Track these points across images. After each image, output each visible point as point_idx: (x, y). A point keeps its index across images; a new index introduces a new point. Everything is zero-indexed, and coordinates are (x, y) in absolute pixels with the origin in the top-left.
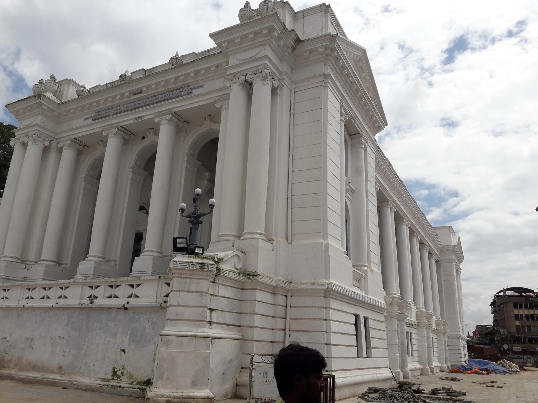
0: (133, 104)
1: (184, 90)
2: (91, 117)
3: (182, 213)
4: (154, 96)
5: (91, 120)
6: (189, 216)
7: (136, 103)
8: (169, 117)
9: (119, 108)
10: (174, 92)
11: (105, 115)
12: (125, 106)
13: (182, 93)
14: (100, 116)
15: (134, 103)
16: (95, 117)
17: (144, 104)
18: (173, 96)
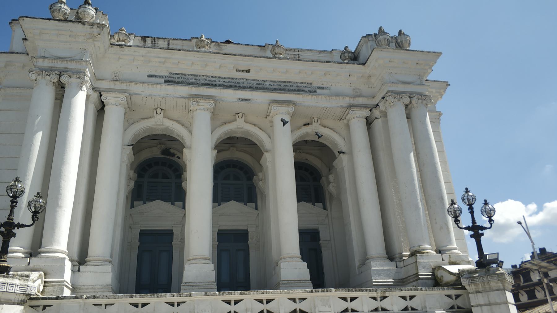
0: (232, 80)
1: (305, 85)
2: (163, 77)
3: (457, 224)
4: (264, 81)
5: (162, 80)
6: (468, 228)
7: (238, 81)
8: (291, 109)
9: (210, 79)
10: (292, 84)
11: (188, 81)
12: (221, 80)
13: (304, 89)
14: (177, 80)
15: (235, 80)
16: (170, 79)
17: (250, 85)
18: (292, 88)
